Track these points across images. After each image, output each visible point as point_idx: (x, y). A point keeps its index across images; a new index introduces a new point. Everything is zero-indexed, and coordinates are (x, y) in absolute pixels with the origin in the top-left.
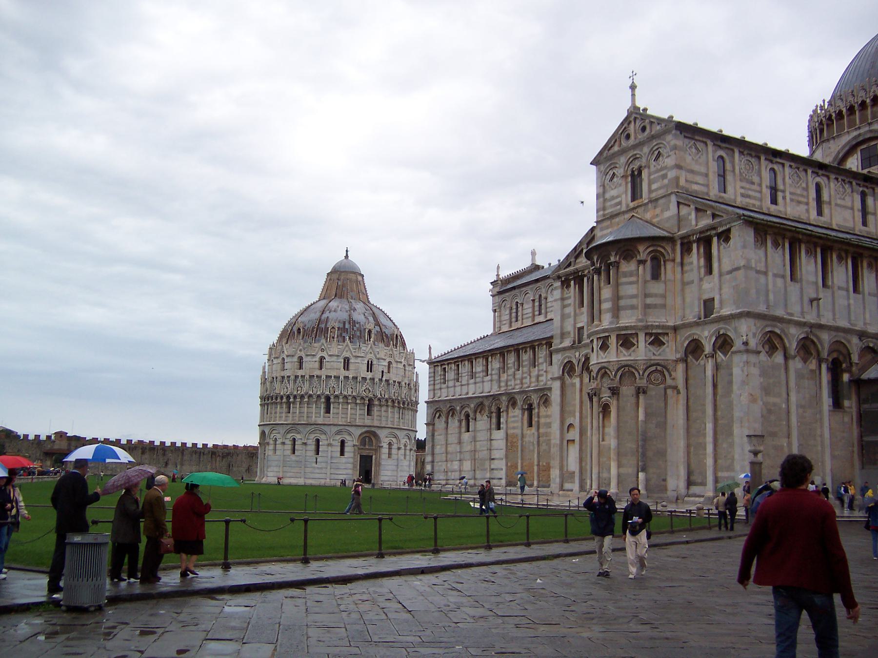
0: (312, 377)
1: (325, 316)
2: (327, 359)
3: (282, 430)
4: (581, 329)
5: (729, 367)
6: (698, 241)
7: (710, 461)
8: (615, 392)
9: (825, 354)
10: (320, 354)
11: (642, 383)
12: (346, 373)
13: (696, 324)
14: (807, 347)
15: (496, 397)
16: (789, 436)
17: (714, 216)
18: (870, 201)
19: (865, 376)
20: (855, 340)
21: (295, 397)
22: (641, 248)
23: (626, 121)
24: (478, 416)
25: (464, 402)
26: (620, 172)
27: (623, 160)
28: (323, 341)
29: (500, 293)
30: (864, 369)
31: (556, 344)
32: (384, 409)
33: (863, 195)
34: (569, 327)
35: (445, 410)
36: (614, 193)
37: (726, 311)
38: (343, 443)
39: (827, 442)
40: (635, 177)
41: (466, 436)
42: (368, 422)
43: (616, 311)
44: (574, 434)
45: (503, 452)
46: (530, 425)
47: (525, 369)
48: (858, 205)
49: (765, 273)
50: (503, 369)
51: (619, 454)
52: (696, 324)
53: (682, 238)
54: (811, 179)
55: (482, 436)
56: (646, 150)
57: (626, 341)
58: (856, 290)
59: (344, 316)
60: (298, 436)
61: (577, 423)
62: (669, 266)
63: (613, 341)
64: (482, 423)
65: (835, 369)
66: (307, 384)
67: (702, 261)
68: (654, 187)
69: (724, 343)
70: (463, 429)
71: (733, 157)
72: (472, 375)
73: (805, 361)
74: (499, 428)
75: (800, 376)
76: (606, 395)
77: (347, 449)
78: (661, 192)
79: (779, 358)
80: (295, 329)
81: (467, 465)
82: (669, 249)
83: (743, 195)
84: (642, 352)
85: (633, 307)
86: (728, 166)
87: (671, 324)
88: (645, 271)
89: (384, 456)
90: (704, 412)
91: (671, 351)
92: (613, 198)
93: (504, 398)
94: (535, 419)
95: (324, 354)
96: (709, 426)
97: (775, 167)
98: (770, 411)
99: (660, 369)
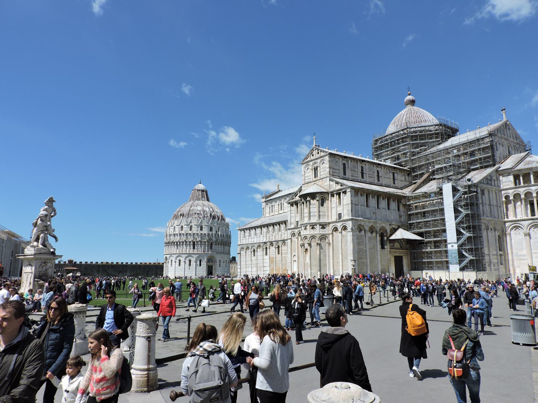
0: (187, 234)
1: (192, 209)
2: (194, 226)
3: (175, 256)
4: (297, 221)
5: (346, 236)
6: (336, 194)
7: (341, 268)
8: (310, 245)
12: (201, 232)
13: (336, 222)
14: (372, 230)
15: (265, 243)
16: (366, 259)
17: (341, 186)
18: (396, 175)
20: (389, 226)
21: (180, 243)
22: (317, 195)
26: (310, 167)
27: (311, 163)
29: (265, 201)
30: (391, 235)
31: (289, 226)
32: (217, 246)
33: (393, 174)
34: (293, 220)
35: (245, 248)
39: (379, 260)
40: (316, 169)
41: (254, 258)
44: (296, 258)
45: (268, 264)
46: (279, 253)
47: (276, 232)
48: (392, 177)
49: (358, 205)
50: (268, 232)
52: (336, 222)
53: (331, 192)
54: (375, 169)
55: (260, 258)
56: (319, 160)
57: (313, 227)
58: (388, 209)
59: (199, 208)
61: (297, 255)
63: (308, 227)
64: (260, 252)
65: (382, 236)
66: (185, 236)
67: (338, 200)
70: (253, 255)
71: (348, 163)
72: (256, 234)
73: (372, 233)
74: (266, 254)
75: (370, 238)
76: (306, 246)
78: (324, 176)
79: (363, 233)
80: (179, 214)
81: (254, 269)
82: (327, 196)
84: (318, 231)
85: (315, 216)
86: (347, 166)
92: (308, 176)
93: (268, 243)
94: (280, 251)
96: (341, 256)
97: (363, 165)
98: (360, 251)
99: (323, 237)
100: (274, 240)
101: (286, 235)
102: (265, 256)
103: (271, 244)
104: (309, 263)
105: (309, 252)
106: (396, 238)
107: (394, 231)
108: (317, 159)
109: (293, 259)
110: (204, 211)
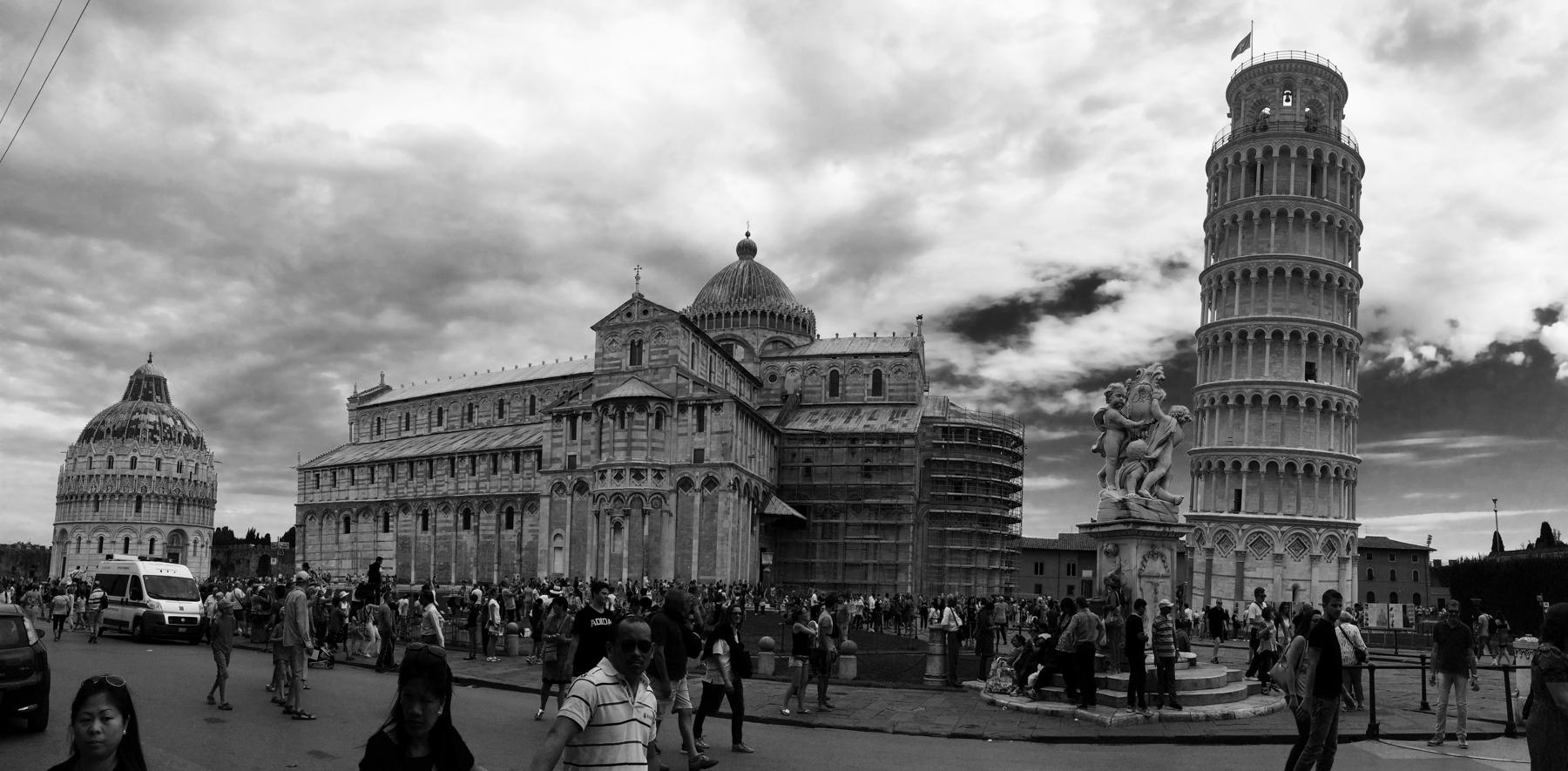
11: (648, 507)
15: (382, 503)
23: (631, 302)
24: (361, 519)
27: (625, 331)
36: (614, 355)
37: (716, 460)
40: (636, 350)
41: (345, 538)
43: (629, 450)
45: (392, 554)
46: (425, 528)
51: (629, 563)
56: (648, 328)
57: (638, 474)
63: (627, 474)
69: (711, 483)
76: (618, 516)
84: (648, 484)
85: (642, 449)
88: (652, 421)
90: (690, 531)
91: (666, 485)
96: (695, 542)
99: (660, 497)
100: (411, 496)
101: (452, 487)
102: (382, 536)
103: (404, 506)
104: (625, 554)
105: (626, 532)
108: (644, 324)
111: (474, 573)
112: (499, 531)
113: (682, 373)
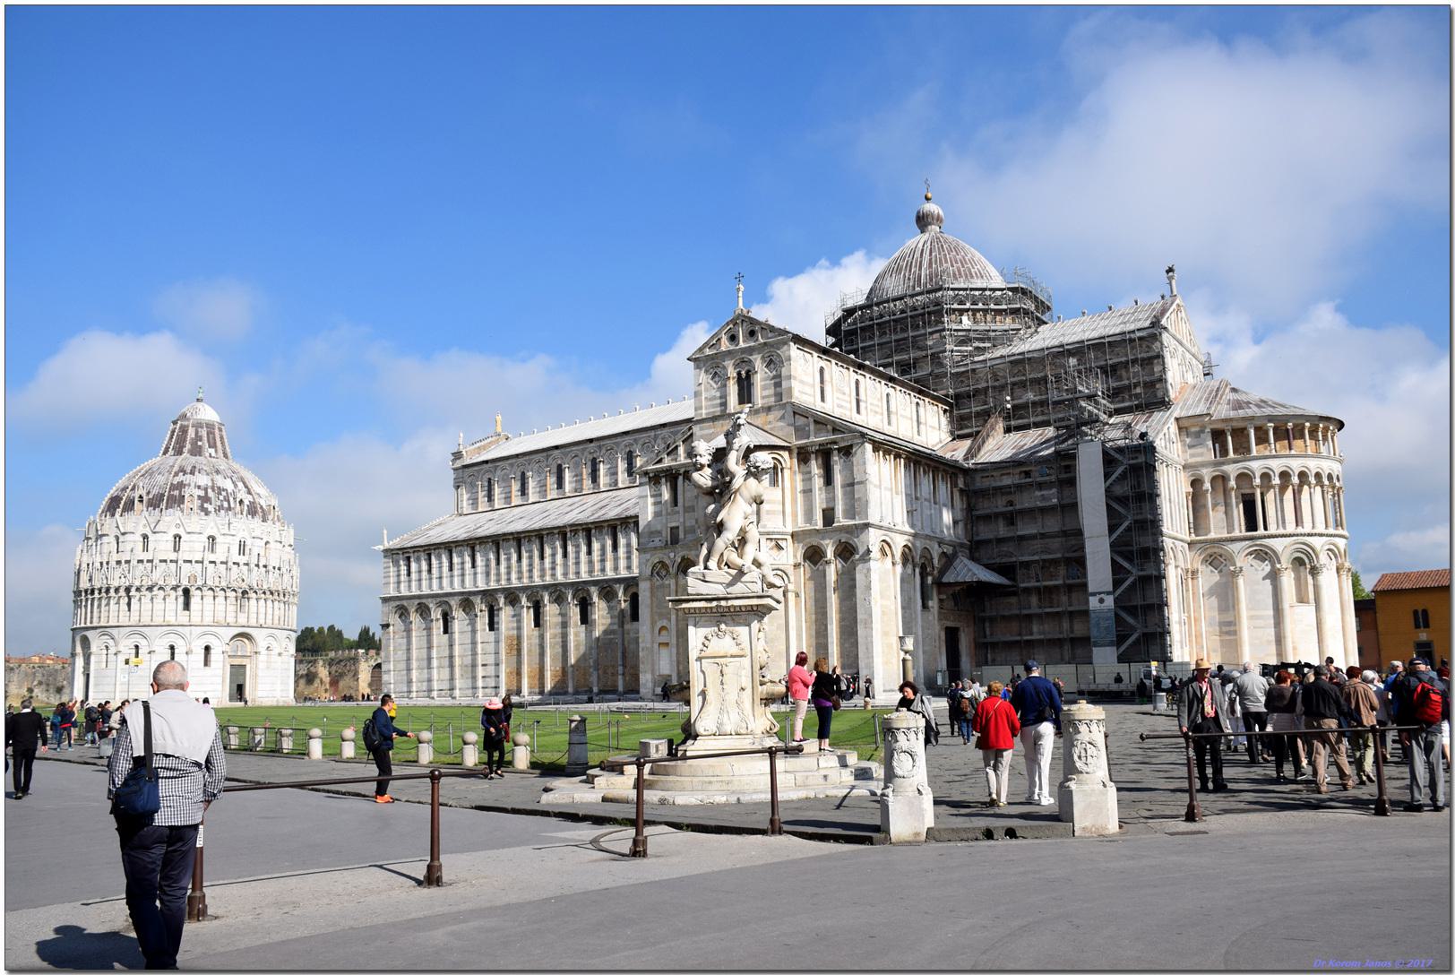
4: (674, 530)
9: (917, 559)
10: (175, 531)
18: (921, 410)
19: (945, 580)
25: (443, 599)
28: (178, 513)
30: (943, 572)
38: (207, 649)
42: (242, 620)
59: (203, 480)
60: (142, 643)
62: (787, 472)
68: (766, 393)
77: (215, 655)
83: (840, 406)
87: (790, 529)
89: (261, 666)
95: (181, 531)
103: (512, 597)
106: (960, 579)
107: (948, 560)
108: (750, 350)
109: (663, 639)
110: (220, 490)
111: (594, 679)
112: (622, 624)
113: (799, 412)
